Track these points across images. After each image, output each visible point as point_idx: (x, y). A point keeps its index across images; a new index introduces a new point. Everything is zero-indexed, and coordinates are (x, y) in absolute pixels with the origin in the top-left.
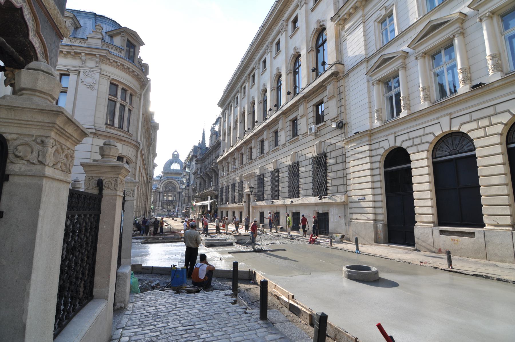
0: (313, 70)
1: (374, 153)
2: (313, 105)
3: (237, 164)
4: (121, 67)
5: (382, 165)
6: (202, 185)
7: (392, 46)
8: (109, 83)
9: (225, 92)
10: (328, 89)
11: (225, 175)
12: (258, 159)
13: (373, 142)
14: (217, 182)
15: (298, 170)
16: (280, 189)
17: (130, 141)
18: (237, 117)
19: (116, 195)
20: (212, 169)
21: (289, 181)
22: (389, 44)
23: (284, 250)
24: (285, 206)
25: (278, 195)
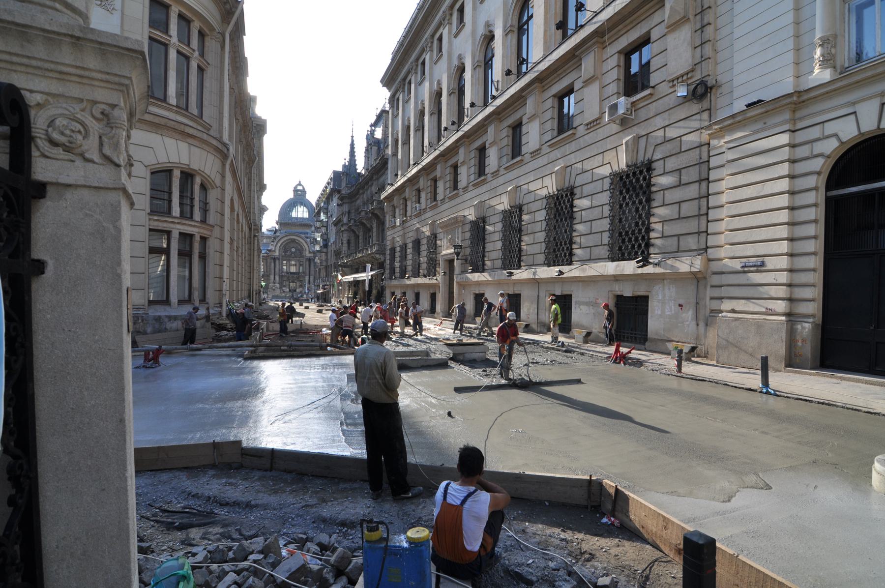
2: (619, 52)
3: (423, 200)
5: (822, 181)
6: (352, 245)
9: (395, 54)
11: (398, 224)
12: (471, 188)
13: (800, 125)
15: (572, 206)
16: (524, 248)
17: (205, 137)
18: (423, 103)
20: (373, 213)
21: (548, 231)
23: (578, 381)
24: (536, 282)
25: (520, 261)
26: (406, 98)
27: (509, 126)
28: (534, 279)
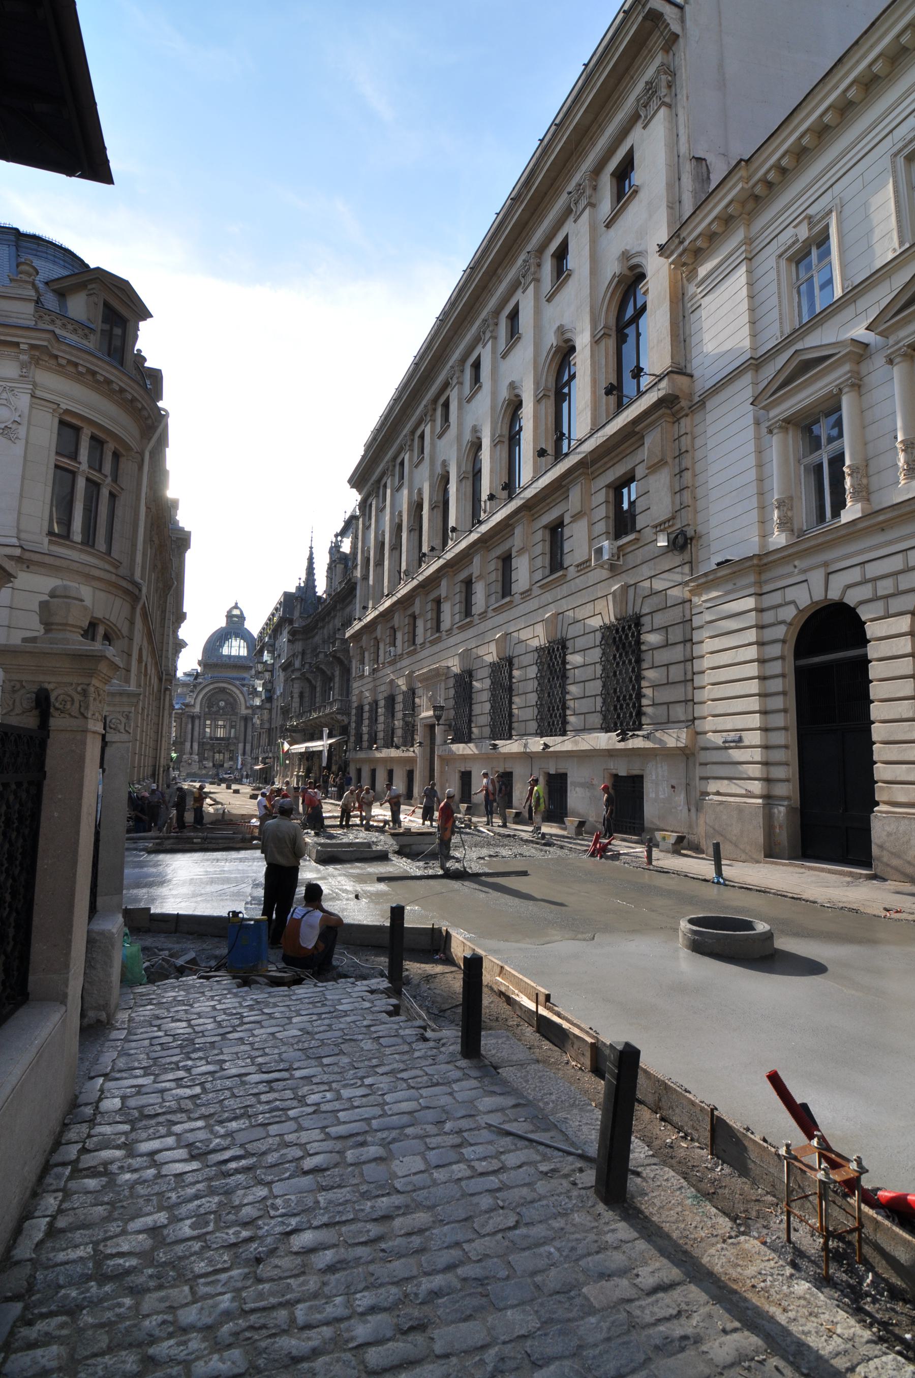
0: (609, 391)
1: (769, 617)
2: (608, 486)
3: (399, 642)
4: (89, 377)
6: (306, 699)
7: (825, 326)
8: (56, 421)
10: (648, 441)
11: (367, 673)
12: (455, 631)
14: (346, 690)
15: (564, 662)
16: (515, 711)
18: (400, 513)
19: (85, 731)
20: (334, 657)
21: (540, 691)
22: (818, 320)
23: (525, 873)
24: (528, 757)
25: (511, 729)
26: (381, 505)
27: (498, 558)
28: (525, 753)
